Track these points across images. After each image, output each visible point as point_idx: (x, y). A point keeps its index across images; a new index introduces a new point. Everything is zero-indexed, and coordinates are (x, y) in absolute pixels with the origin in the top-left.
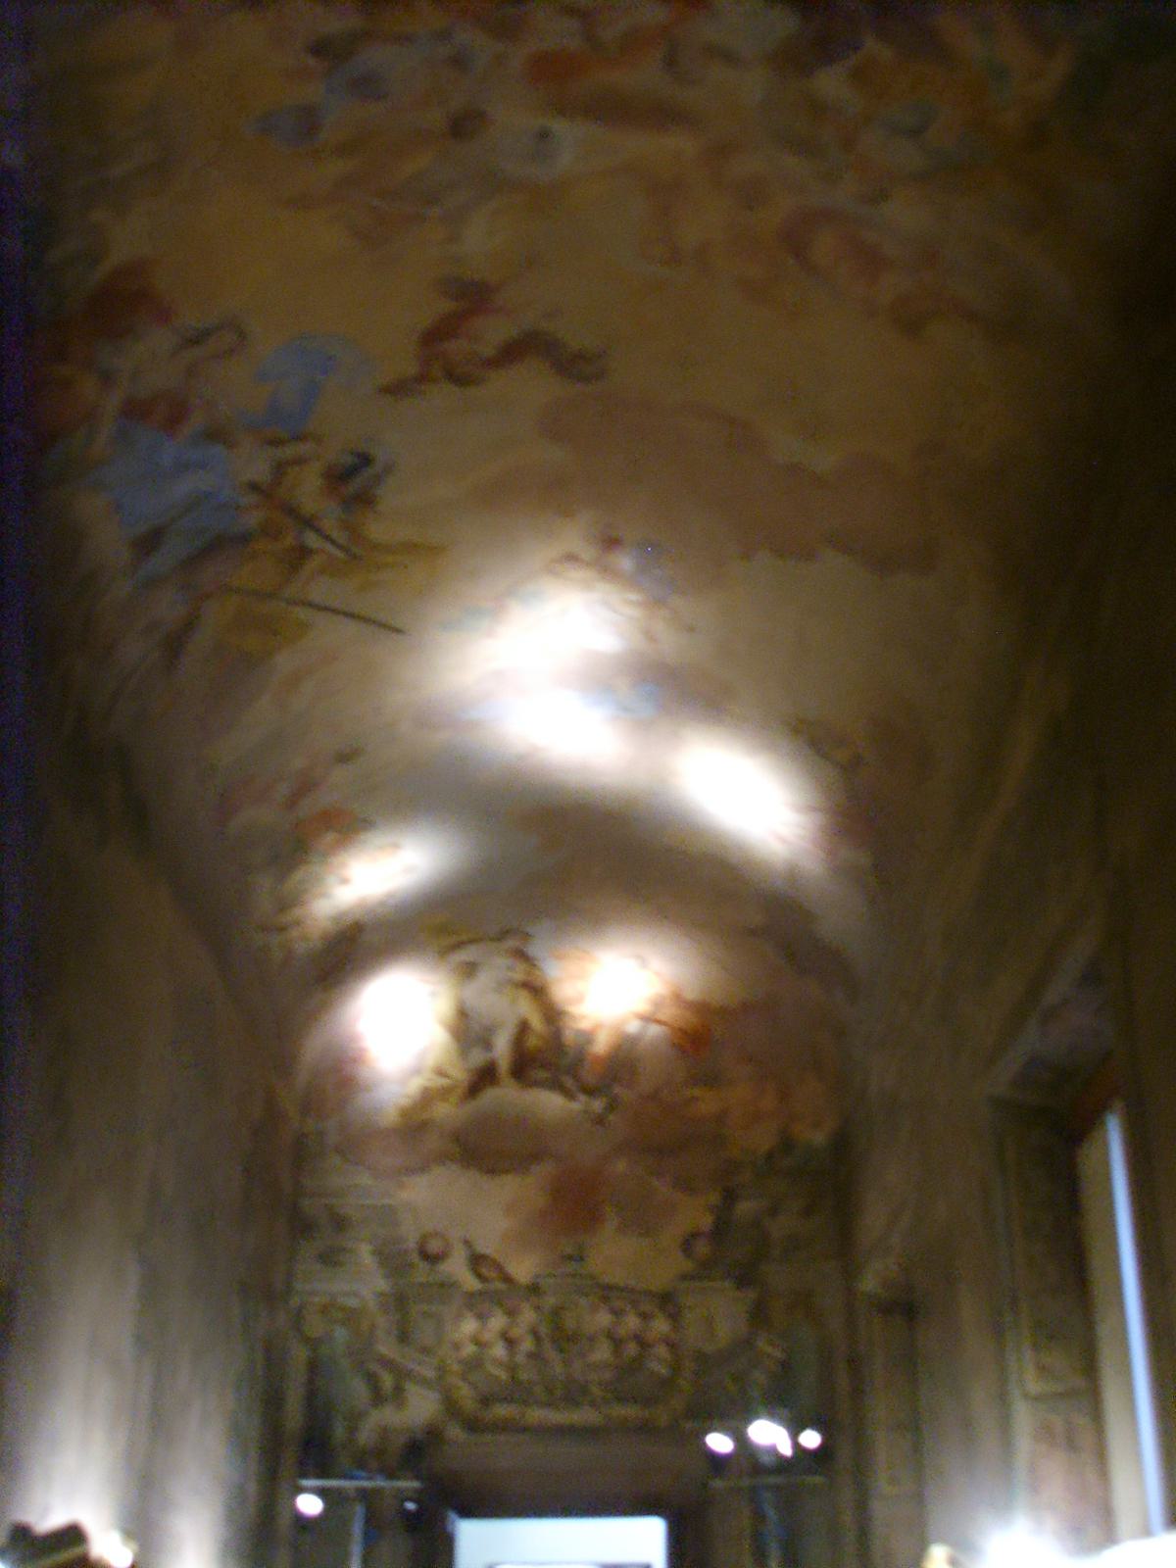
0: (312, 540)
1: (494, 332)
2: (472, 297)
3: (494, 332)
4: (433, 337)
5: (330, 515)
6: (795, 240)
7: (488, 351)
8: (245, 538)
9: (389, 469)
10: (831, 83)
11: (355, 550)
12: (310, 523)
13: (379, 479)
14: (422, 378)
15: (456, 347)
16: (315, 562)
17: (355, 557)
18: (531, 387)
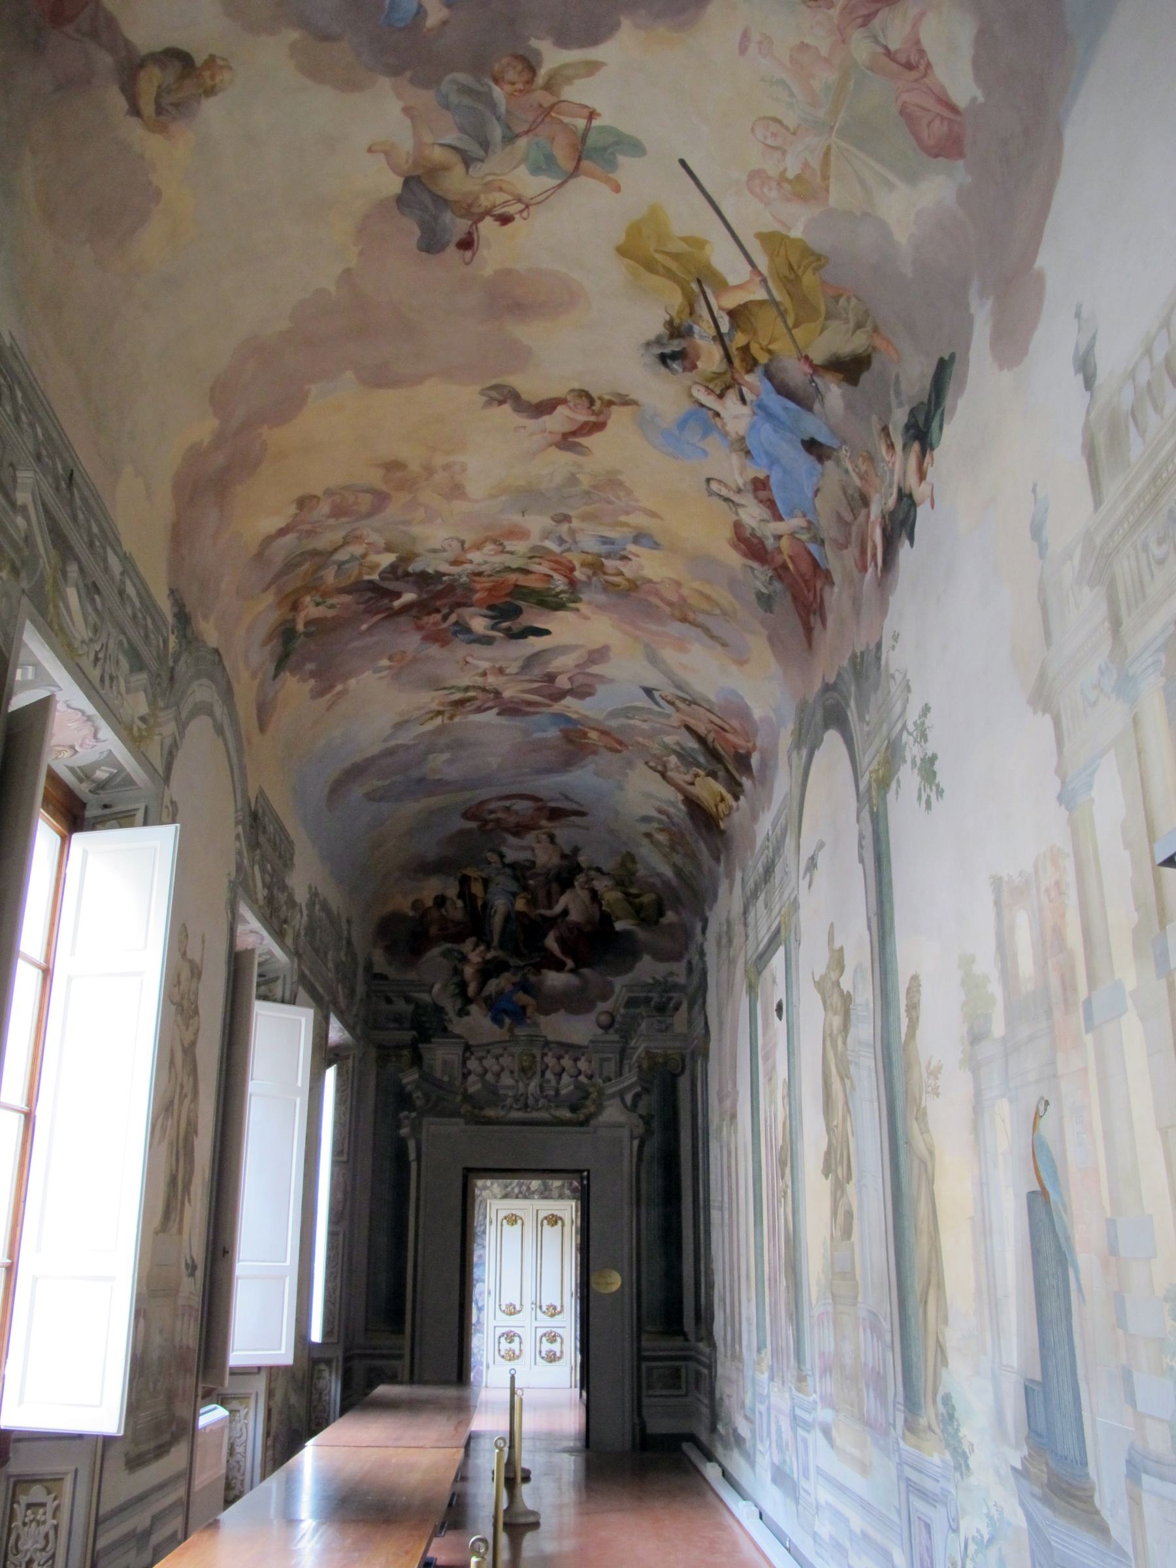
0: (725, 327)
1: (559, 421)
2: (568, 441)
3: (559, 421)
4: (599, 426)
5: (703, 331)
6: (381, 499)
7: (561, 410)
8: (769, 375)
9: (648, 344)
10: (387, 559)
11: (695, 286)
12: (720, 338)
13: (658, 341)
14: (610, 403)
15: (582, 417)
16: (732, 301)
17: (699, 282)
18: (532, 387)
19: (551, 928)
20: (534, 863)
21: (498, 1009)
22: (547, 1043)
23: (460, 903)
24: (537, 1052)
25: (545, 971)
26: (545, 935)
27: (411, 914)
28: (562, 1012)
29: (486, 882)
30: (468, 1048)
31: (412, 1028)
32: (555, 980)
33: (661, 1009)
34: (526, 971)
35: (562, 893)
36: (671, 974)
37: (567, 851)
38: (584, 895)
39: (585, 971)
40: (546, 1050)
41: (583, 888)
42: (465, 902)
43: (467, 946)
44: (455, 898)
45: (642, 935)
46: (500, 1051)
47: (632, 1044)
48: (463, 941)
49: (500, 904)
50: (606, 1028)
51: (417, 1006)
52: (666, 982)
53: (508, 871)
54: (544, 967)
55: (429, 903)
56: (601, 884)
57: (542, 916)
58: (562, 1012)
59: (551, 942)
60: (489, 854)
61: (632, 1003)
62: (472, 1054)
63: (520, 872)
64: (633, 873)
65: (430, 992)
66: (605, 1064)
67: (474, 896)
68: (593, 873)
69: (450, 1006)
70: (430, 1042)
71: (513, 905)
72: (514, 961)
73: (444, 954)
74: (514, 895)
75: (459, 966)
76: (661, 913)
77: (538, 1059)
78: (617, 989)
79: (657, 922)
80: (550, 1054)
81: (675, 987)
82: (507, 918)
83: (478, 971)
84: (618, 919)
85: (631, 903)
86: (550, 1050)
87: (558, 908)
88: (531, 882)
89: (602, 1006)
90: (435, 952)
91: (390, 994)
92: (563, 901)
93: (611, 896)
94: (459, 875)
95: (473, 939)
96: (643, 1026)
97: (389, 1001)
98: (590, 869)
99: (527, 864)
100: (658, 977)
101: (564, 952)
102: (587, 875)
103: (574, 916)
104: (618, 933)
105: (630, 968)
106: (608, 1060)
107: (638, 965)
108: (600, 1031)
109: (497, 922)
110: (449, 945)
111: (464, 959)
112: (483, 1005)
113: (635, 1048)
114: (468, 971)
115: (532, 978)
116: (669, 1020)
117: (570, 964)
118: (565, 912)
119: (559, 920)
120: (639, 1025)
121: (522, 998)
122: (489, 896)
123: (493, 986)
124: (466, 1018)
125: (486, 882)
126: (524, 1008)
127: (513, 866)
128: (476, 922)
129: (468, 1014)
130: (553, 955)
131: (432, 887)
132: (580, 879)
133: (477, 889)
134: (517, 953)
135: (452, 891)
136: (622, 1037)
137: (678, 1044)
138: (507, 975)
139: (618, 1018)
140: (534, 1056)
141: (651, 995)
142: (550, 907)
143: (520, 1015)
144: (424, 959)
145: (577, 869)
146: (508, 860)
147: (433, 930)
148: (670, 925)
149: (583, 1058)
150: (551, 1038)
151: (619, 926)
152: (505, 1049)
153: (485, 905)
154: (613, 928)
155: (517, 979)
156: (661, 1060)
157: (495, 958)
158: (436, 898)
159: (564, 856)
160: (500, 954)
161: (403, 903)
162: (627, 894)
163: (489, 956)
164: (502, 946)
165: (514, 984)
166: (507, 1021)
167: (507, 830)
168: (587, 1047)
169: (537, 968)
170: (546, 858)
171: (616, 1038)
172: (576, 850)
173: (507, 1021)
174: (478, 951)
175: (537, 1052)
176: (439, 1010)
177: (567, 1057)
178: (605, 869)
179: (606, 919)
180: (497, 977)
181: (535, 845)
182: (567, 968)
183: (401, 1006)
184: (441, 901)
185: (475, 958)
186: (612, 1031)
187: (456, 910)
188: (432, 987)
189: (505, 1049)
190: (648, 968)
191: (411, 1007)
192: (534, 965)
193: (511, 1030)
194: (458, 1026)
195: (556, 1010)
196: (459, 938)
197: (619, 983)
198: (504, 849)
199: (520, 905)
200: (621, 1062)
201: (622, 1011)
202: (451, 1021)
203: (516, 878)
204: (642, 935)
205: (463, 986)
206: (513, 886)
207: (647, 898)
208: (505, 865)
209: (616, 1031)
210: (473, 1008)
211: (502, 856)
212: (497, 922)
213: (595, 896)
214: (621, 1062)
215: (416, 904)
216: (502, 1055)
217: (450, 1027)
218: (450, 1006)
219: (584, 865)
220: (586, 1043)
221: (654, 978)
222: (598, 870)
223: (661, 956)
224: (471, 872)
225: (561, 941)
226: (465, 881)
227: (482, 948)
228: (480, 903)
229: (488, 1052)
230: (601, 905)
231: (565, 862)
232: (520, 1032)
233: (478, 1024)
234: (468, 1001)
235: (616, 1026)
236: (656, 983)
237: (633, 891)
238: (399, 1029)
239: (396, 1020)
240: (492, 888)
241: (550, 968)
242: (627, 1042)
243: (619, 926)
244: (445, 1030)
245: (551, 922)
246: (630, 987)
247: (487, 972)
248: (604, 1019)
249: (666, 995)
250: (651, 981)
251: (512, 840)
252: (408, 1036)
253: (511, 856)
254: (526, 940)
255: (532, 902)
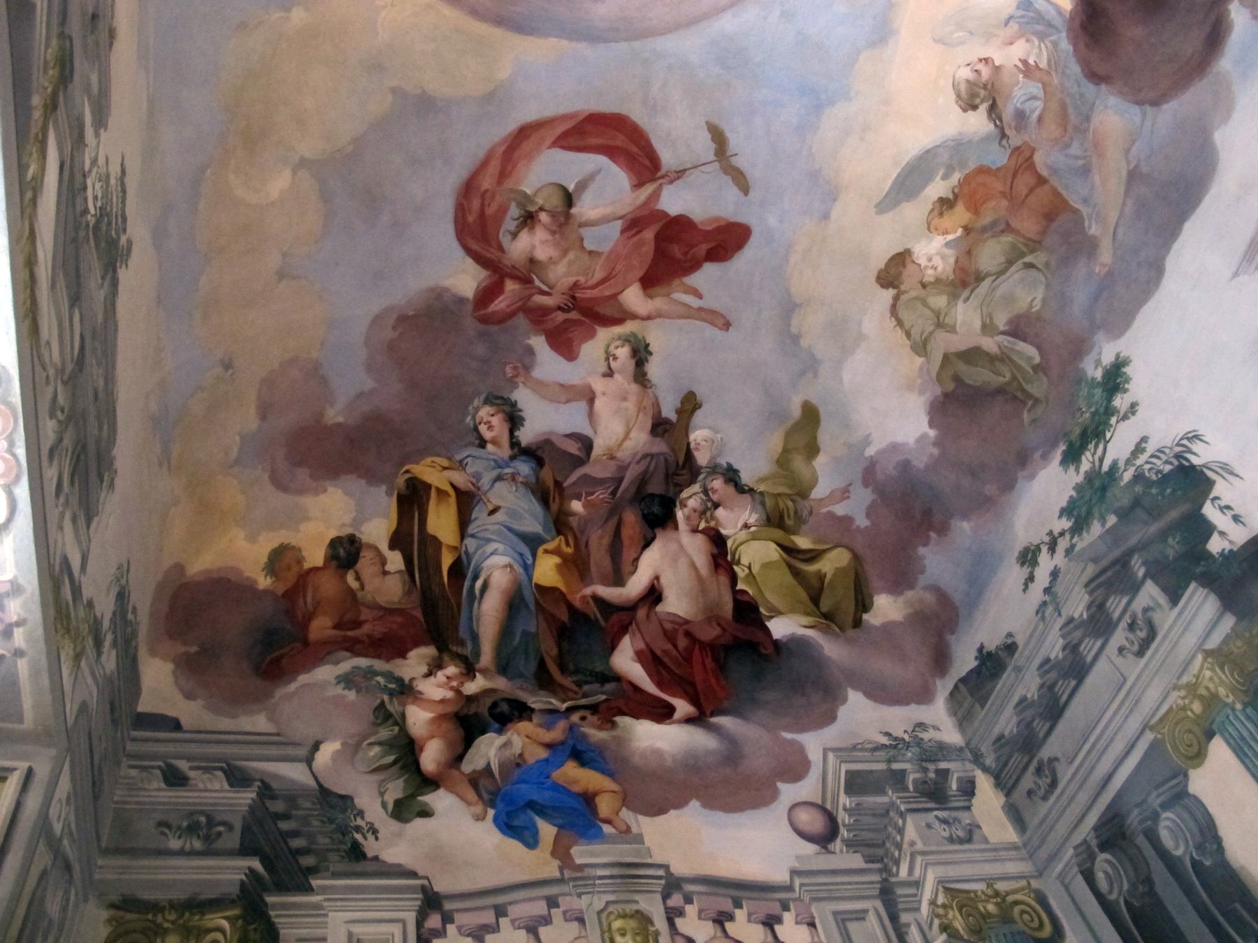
19: (624, 630)
20: (587, 444)
21: (513, 805)
22: (673, 884)
23: (395, 561)
24: (654, 908)
25: (624, 721)
26: (613, 648)
27: (264, 582)
28: (695, 804)
29: (466, 501)
30: (431, 901)
31: (246, 850)
32: (652, 738)
33: (934, 793)
34: (575, 718)
35: (647, 544)
36: (921, 726)
37: (669, 412)
38: (696, 548)
39: (723, 721)
40: (676, 900)
41: (695, 531)
42: (408, 561)
43: (413, 665)
44: (384, 546)
45: (832, 649)
46: (540, 908)
47: (903, 872)
48: (403, 654)
49: (497, 568)
50: (825, 838)
51: (266, 791)
52: (919, 742)
53: (524, 468)
54: (623, 713)
55: (316, 556)
56: (735, 520)
57: (598, 600)
58: (695, 804)
59: (626, 660)
60: (485, 412)
61: (855, 784)
62: (447, 918)
63: (551, 469)
64: (802, 493)
65: (309, 761)
66: (853, 927)
67: (437, 543)
68: (717, 483)
69: (371, 798)
70: (309, 890)
71: (528, 569)
72: (537, 701)
73: (347, 680)
74: (533, 542)
75: (393, 707)
76: (863, 604)
77: (660, 924)
78: (814, 755)
79: (857, 623)
80: (691, 910)
81: (942, 750)
82: (514, 604)
83: (441, 717)
84: (776, 613)
85: (796, 573)
86: (688, 900)
87: (636, 584)
88: (577, 506)
89: (789, 792)
90: (325, 673)
91: (183, 765)
92: (651, 564)
93: (757, 555)
94: (401, 481)
95: (429, 651)
96: (911, 833)
97: (175, 779)
98: (714, 469)
99: (573, 448)
100: (899, 732)
101: (660, 684)
102: (705, 491)
103: (676, 604)
104: (776, 644)
105: (830, 718)
106: (860, 916)
107: (842, 712)
108: (810, 848)
109: (490, 610)
110: (363, 662)
111: (405, 690)
112: (471, 795)
113: (917, 884)
114: (418, 718)
115: (596, 735)
116: (965, 818)
117: (683, 707)
118: (654, 594)
119: (641, 613)
120: (901, 831)
121: (573, 774)
122: (470, 543)
123: (488, 750)
124: (419, 824)
125: (466, 501)
126: (589, 799)
127: (534, 454)
128: (436, 612)
129: (426, 813)
130: (636, 689)
131: (334, 511)
132: (692, 498)
133: (441, 522)
134: (544, 681)
135: (377, 530)
136: (869, 859)
137: (1012, 868)
138: (524, 726)
139: (843, 817)
140: (644, 920)
141: (895, 766)
142: (618, 579)
143: (580, 817)
144: (293, 687)
145: (683, 468)
146: (526, 435)
147: (321, 627)
148: (888, 628)
149: (788, 917)
150: (680, 868)
151: (780, 628)
152: (552, 902)
153: (458, 570)
154: (767, 631)
155: (557, 733)
156: (991, 908)
157: (487, 692)
158: (335, 543)
159: (660, 427)
160: (501, 683)
161: (245, 552)
162: (790, 550)
163: (471, 688)
164: (503, 667)
165: (549, 746)
166: (547, 831)
167: (538, 317)
168: (790, 888)
169: (606, 714)
170: (619, 433)
171: (856, 861)
172: (690, 404)
173: (547, 831)
174: (441, 676)
175: (654, 908)
176: (333, 802)
177: (740, 915)
178: (746, 478)
179: (748, 612)
180: (500, 732)
181: (599, 385)
182: (677, 716)
183: (212, 791)
184: (346, 552)
185: (435, 689)
186: (837, 845)
187: (385, 579)
188: (316, 747)
189: (552, 902)
190: (862, 717)
191: (247, 797)
192: (594, 708)
193: (561, 852)
194: (397, 845)
195: (680, 804)
196: (393, 647)
197: (814, 743)
198: (523, 397)
199: (547, 570)
200: (894, 918)
201: (844, 800)
202: (375, 832)
203: (543, 495)
204: (832, 649)
205: (407, 750)
206: (532, 518)
207: (833, 563)
208: (521, 451)
209: (849, 844)
210: (440, 800)
211: (514, 420)
212: (490, 610)
213: (720, 553)
214: (894, 918)
215: (280, 558)
216: (547, 920)
217: (370, 847)
218: (371, 798)
219: (702, 458)
220: (780, 876)
221: (887, 734)
222: (731, 476)
223: (882, 693)
224: (430, 472)
225: (650, 659)
226: (413, 499)
227: (452, 670)
228: (447, 561)
229: (500, 911)
230: (734, 579)
231: (660, 446)
232: (582, 853)
233: (459, 838)
234: (431, 783)
235: (844, 833)
236: (896, 745)
237: (803, 542)
238: (206, 853)
239: (193, 829)
240: (480, 520)
241: (637, 716)
242: (885, 869)
243: (780, 628)
244: (357, 853)
245: (619, 618)
246: (847, 752)
247: (467, 723)
248: (811, 820)
249: (931, 767)
250: (885, 740)
251: (549, 364)
252: (230, 872)
253: (543, 419)
254: (567, 642)
255: (576, 565)
